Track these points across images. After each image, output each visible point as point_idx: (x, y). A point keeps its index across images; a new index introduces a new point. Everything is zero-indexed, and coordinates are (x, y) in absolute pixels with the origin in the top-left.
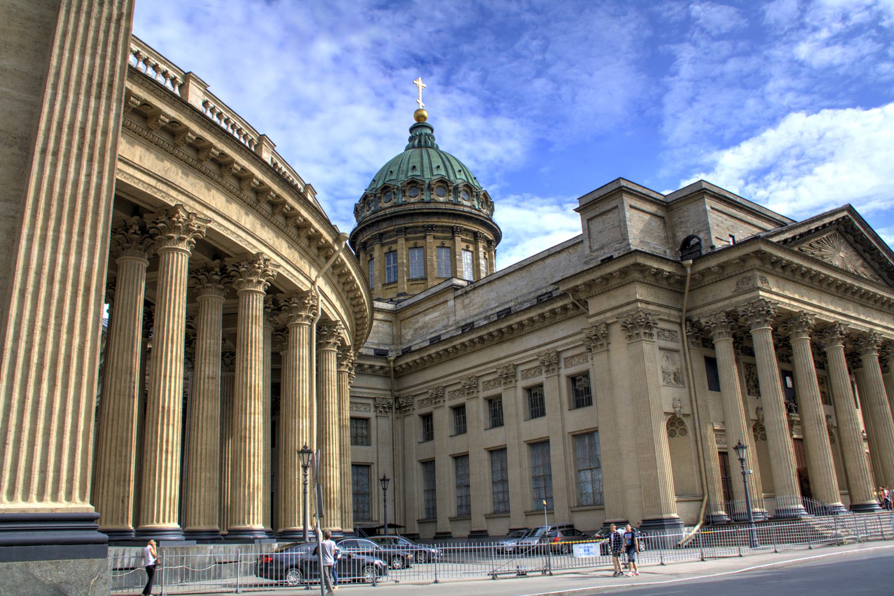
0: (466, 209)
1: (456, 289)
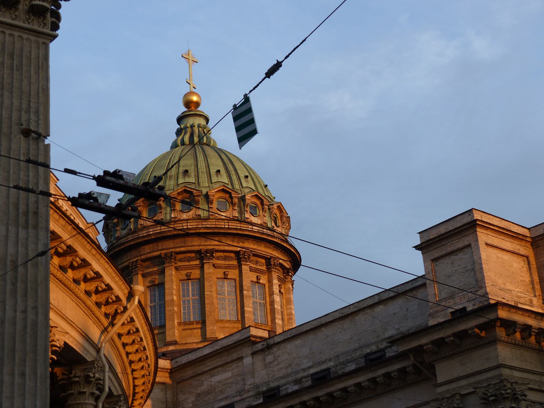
1: (255, 343)
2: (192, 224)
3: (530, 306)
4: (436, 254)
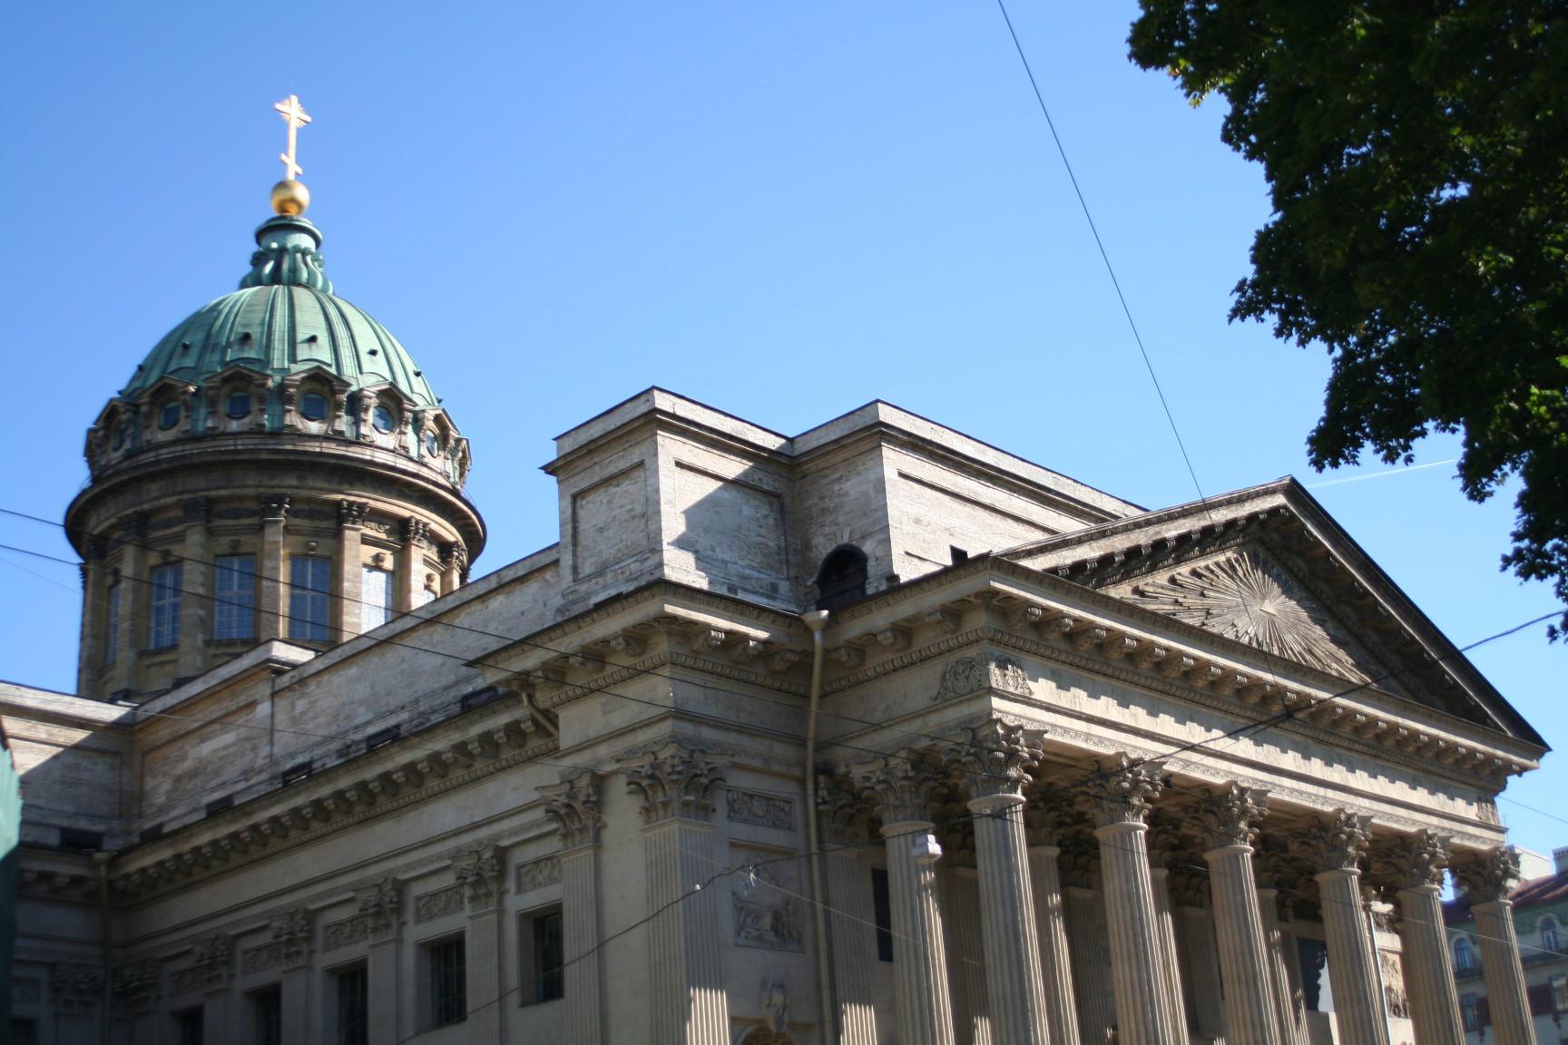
0: (382, 457)
1: (279, 673)
2: (247, 441)
3: (768, 597)
4: (582, 482)
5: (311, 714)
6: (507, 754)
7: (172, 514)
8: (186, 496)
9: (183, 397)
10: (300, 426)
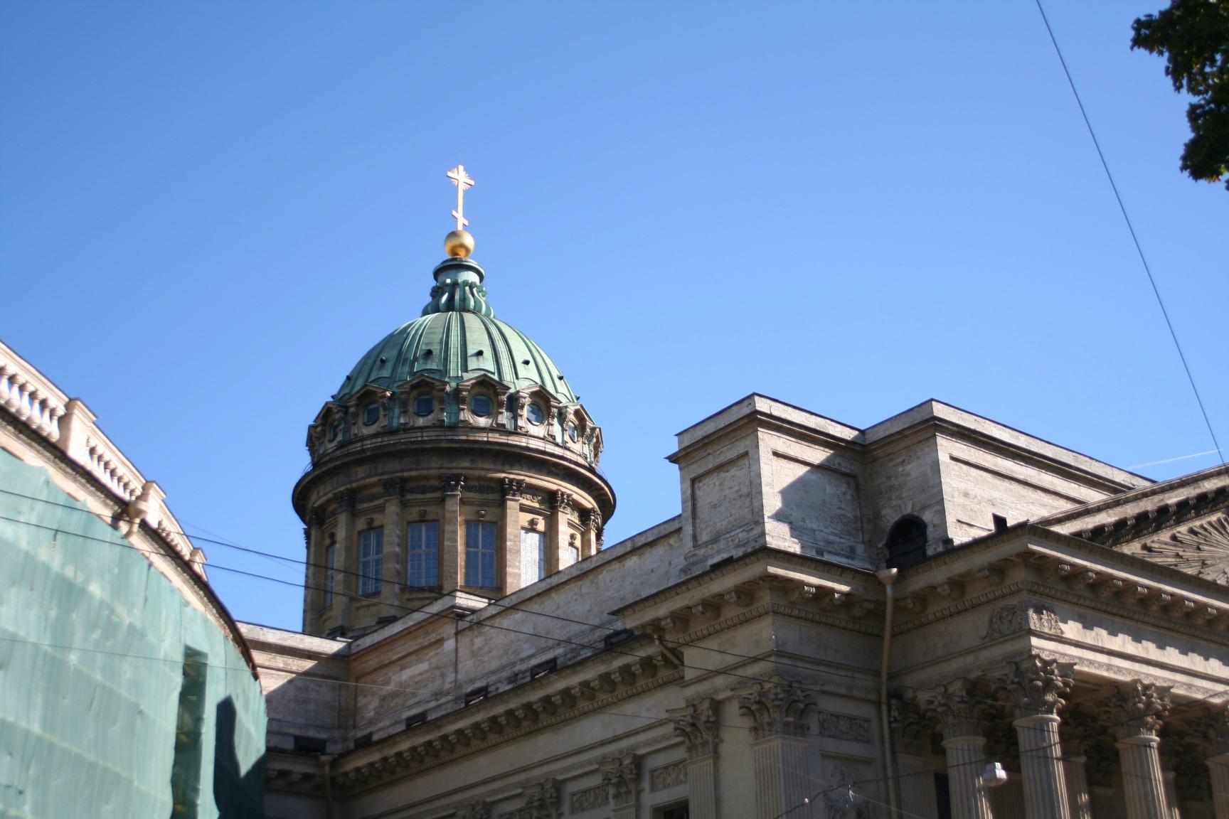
0: (534, 444)
2: (431, 434)
3: (848, 557)
5: (486, 649)
6: (642, 683)
7: (374, 490)
8: (385, 477)
9: (381, 400)
10: (471, 421)
